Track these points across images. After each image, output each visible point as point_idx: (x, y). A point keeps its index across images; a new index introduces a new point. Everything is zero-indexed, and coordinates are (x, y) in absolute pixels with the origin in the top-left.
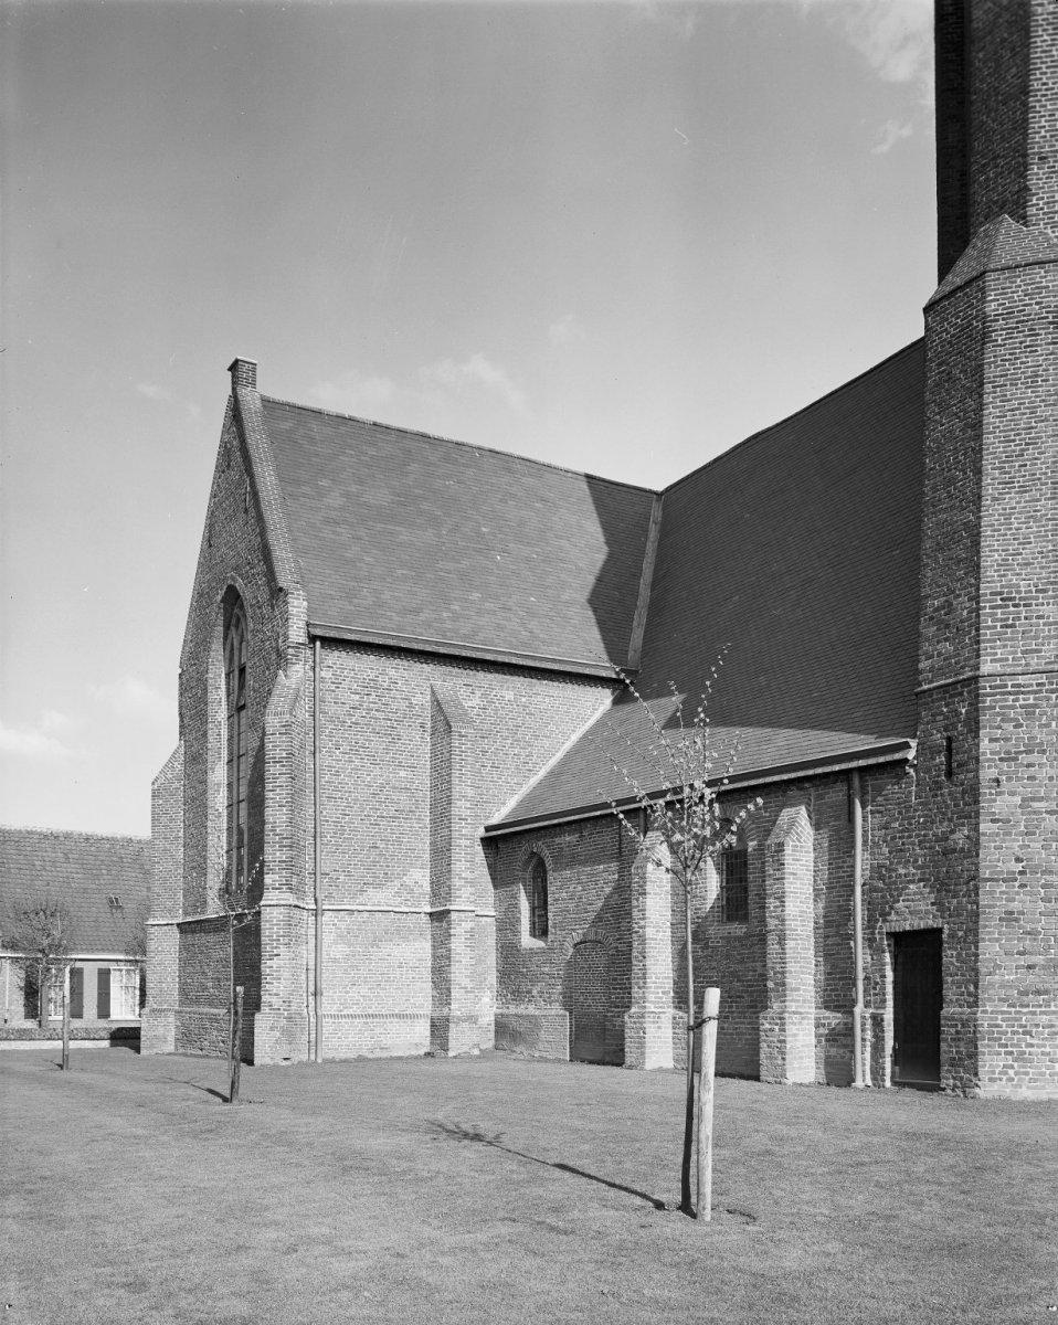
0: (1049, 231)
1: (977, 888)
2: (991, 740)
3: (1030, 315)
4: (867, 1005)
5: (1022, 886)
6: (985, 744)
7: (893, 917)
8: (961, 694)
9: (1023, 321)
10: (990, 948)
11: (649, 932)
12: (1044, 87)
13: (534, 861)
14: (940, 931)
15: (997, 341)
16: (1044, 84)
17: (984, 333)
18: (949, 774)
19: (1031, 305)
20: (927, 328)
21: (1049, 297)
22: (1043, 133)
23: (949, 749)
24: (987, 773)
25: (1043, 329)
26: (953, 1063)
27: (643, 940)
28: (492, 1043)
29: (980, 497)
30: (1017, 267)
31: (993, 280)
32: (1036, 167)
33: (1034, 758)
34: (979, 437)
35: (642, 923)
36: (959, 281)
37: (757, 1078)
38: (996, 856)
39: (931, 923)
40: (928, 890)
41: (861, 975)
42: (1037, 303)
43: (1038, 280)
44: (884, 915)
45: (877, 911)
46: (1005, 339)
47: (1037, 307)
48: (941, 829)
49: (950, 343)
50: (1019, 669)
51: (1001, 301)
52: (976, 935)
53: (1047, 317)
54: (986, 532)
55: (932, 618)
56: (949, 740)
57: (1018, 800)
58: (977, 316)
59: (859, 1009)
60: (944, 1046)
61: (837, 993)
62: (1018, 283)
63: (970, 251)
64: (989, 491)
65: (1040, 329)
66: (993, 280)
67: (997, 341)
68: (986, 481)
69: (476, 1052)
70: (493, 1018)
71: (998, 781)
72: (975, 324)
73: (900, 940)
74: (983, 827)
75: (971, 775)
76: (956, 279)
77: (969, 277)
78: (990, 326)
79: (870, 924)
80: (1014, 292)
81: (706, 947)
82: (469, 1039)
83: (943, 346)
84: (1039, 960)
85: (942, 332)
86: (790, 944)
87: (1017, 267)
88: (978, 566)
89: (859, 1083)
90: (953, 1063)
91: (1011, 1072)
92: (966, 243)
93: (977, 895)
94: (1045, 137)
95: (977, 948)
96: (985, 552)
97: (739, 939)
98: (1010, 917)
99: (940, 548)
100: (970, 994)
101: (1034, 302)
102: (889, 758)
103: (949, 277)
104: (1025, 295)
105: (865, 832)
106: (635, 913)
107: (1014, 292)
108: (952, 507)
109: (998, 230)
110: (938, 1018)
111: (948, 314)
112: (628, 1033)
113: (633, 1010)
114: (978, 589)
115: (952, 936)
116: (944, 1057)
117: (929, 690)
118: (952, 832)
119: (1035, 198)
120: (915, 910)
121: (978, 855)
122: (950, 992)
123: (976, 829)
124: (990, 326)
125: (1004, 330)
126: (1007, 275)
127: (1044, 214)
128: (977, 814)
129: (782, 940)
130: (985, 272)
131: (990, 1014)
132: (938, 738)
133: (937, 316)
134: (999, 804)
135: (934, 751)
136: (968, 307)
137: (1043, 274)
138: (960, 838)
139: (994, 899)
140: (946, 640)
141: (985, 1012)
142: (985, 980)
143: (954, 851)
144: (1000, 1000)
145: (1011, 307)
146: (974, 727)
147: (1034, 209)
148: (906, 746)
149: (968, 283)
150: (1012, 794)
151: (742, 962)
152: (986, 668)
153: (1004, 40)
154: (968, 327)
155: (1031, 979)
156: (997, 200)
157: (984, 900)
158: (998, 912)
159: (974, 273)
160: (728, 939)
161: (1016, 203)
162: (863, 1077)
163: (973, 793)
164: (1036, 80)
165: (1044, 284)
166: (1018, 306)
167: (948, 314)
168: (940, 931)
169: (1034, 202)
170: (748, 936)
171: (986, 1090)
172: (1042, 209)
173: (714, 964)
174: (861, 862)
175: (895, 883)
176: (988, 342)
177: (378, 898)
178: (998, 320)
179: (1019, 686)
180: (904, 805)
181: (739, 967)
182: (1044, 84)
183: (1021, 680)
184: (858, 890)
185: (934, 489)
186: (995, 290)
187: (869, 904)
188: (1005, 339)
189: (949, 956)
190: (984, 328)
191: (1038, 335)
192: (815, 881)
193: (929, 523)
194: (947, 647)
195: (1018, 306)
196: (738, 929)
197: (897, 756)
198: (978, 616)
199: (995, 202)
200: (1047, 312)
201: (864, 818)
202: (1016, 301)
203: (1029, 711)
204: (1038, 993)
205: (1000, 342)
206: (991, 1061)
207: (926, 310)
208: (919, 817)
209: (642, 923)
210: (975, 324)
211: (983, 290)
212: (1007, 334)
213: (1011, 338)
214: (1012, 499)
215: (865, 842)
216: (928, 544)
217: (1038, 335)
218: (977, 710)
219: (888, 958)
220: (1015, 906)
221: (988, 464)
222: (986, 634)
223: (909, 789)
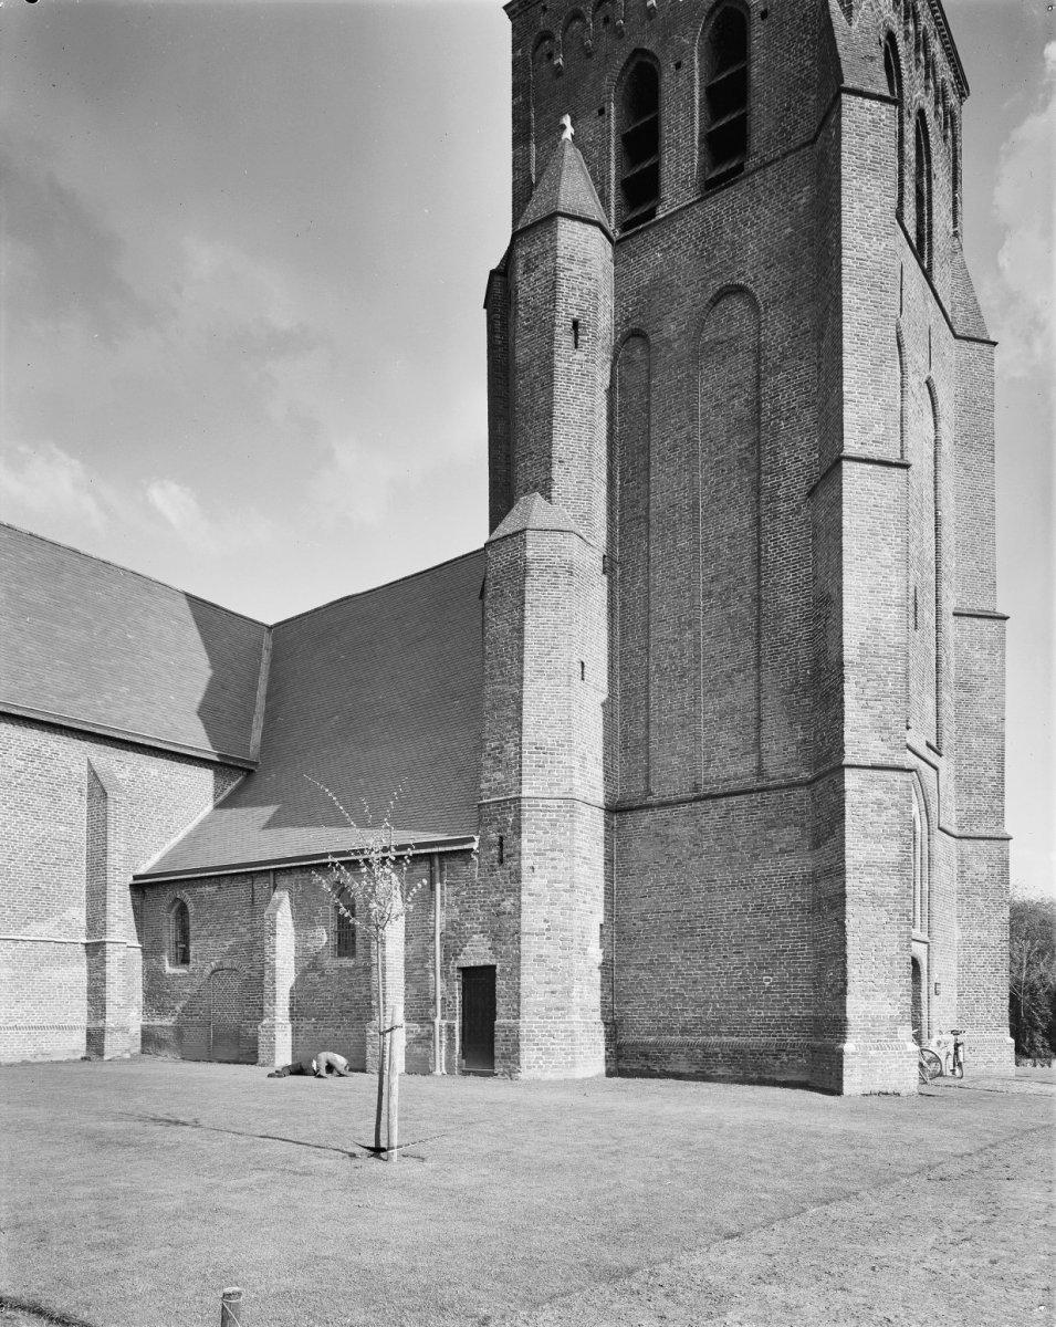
1: (519, 938)
2: (529, 841)
4: (443, 1017)
5: (548, 938)
6: (525, 844)
7: (462, 957)
8: (510, 808)
10: (527, 980)
11: (278, 963)
13: (177, 905)
14: (494, 967)
18: (501, 861)
23: (501, 844)
24: (526, 863)
26: (504, 1057)
27: (273, 970)
28: (139, 1048)
29: (522, 678)
33: (556, 854)
34: (521, 638)
35: (273, 956)
37: (364, 1071)
38: (531, 919)
39: (488, 962)
40: (486, 939)
41: (439, 997)
44: (456, 955)
45: (450, 953)
48: (494, 899)
50: (546, 795)
52: (519, 970)
54: (526, 702)
55: (489, 755)
56: (501, 838)
57: (545, 881)
59: (438, 1021)
60: (497, 1045)
61: (419, 1011)
64: (527, 676)
68: (526, 668)
69: (127, 1056)
70: (139, 1029)
71: (533, 868)
73: (467, 972)
74: (523, 899)
75: (515, 863)
79: (446, 960)
81: (322, 975)
82: (123, 1043)
84: (559, 987)
86: (388, 974)
88: (521, 724)
89: (438, 1072)
90: (504, 1057)
91: (541, 1062)
93: (519, 943)
95: (519, 979)
96: (525, 715)
97: (349, 970)
98: (540, 959)
99: (494, 708)
100: (514, 1010)
102: (460, 847)
105: (442, 897)
106: (267, 948)
108: (503, 682)
110: (493, 1026)
112: (261, 1039)
113: (265, 1022)
114: (521, 740)
115: (503, 971)
116: (497, 1053)
117: (488, 803)
118: (503, 900)
120: (477, 953)
121: (520, 917)
122: (500, 1009)
123: (519, 899)
128: (520, 889)
129: (384, 969)
131: (528, 1023)
132: (494, 837)
134: (532, 883)
135: (490, 846)
138: (507, 905)
139: (530, 947)
140: (500, 770)
141: (524, 1022)
142: (524, 1001)
143: (504, 913)
144: (534, 1014)
146: (518, 832)
148: (472, 840)
150: (542, 877)
151: (351, 986)
152: (525, 793)
155: (553, 1000)
157: (524, 947)
158: (533, 955)
160: (340, 969)
162: (440, 1069)
163: (516, 876)
168: (494, 967)
170: (355, 967)
171: (525, 1074)
173: (329, 988)
174: (440, 919)
175: (463, 933)
177: (39, 930)
179: (547, 806)
180: (470, 881)
181: (348, 990)
183: (547, 802)
184: (438, 938)
185: (492, 667)
187: (446, 949)
189: (501, 985)
192: (406, 929)
193: (488, 689)
194: (499, 776)
196: (348, 962)
197: (466, 847)
198: (521, 757)
201: (442, 888)
203: (553, 824)
204: (558, 1009)
206: (528, 1055)
208: (481, 889)
209: (273, 956)
214: (542, 682)
215: (442, 904)
216: (488, 704)
218: (520, 820)
219: (457, 985)
220: (542, 952)
221: (527, 657)
222: (525, 770)
223: (474, 870)
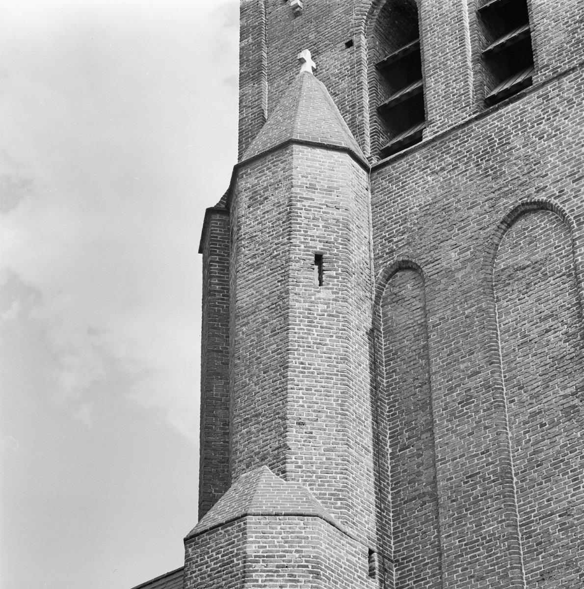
0: (308, 488)
3: (290, 561)
9: (283, 567)
12: (301, 366)
15: (257, 581)
16: (302, 363)
17: (244, 572)
19: (291, 552)
20: (188, 559)
21: (308, 547)
22: (301, 403)
25: (303, 576)
30: (276, 515)
31: (254, 523)
32: (294, 430)
36: (221, 519)
42: (297, 551)
43: (297, 530)
46: (266, 581)
47: (297, 555)
49: (209, 576)
51: (261, 544)
53: (307, 566)
58: (237, 555)
62: (279, 530)
63: (230, 492)
65: (300, 576)
66: (254, 523)
67: (257, 581)
72: (236, 562)
76: (217, 515)
77: (229, 517)
78: (251, 566)
80: (273, 538)
83: (202, 579)
85: (202, 565)
87: (276, 515)
92: (227, 486)
94: (303, 406)
101: (294, 549)
103: (211, 514)
104: (286, 542)
107: (273, 538)
109: (258, 478)
111: (209, 548)
119: (293, 457)
124: (251, 566)
125: (264, 571)
126: (268, 521)
127: (302, 472)
130: (246, 515)
133: (198, 548)
136: (229, 544)
137: (302, 525)
145: (271, 552)
147: (293, 465)
149: (230, 522)
153: (265, 322)
154: (228, 564)
156: (259, 453)
159: (236, 515)
161: (276, 457)
164: (294, 358)
165: (303, 534)
166: (278, 551)
167: (209, 548)
169: (294, 460)
172: (300, 467)
176: (249, 581)
178: (257, 562)
182: (302, 363)
186: (256, 532)
188: (266, 581)
190: (245, 567)
191: (298, 581)
195: (278, 551)
199: (257, 454)
200: (306, 561)
202: (276, 546)
205: (260, 583)
207: (186, 540)
210: (236, 562)
211: (243, 530)
212: (268, 576)
213: (271, 580)
217: (298, 581)
